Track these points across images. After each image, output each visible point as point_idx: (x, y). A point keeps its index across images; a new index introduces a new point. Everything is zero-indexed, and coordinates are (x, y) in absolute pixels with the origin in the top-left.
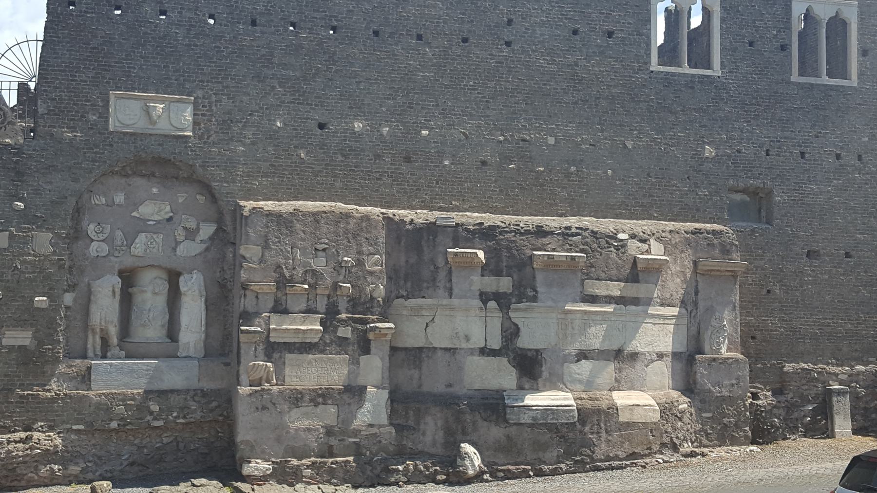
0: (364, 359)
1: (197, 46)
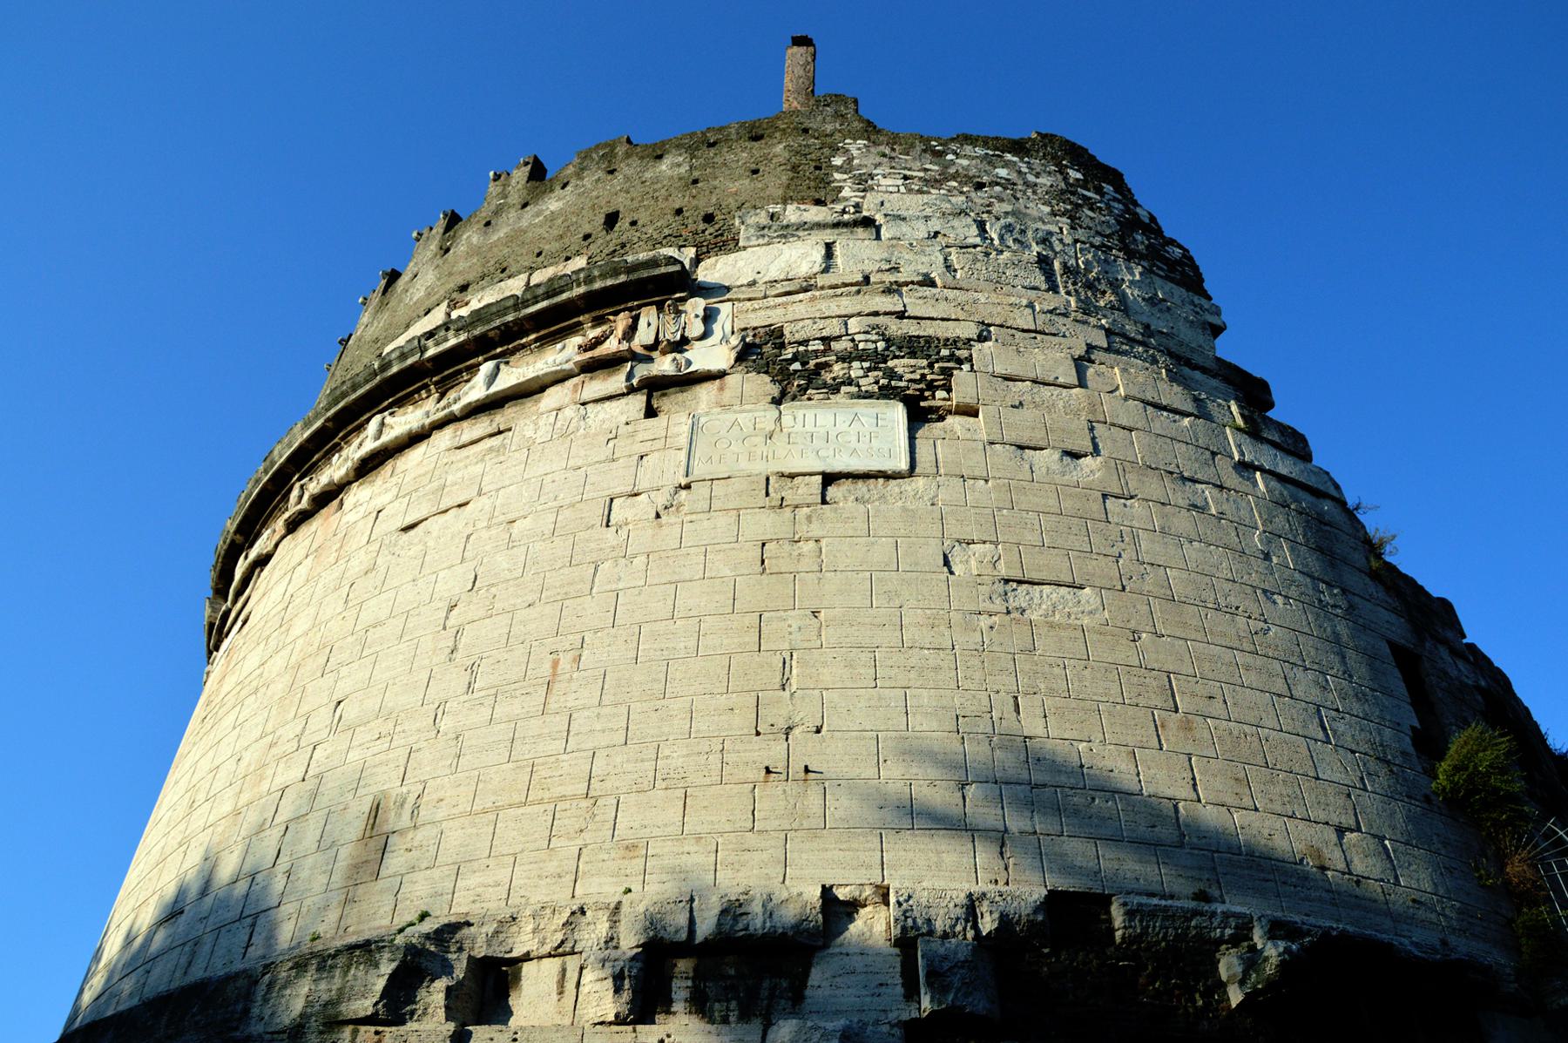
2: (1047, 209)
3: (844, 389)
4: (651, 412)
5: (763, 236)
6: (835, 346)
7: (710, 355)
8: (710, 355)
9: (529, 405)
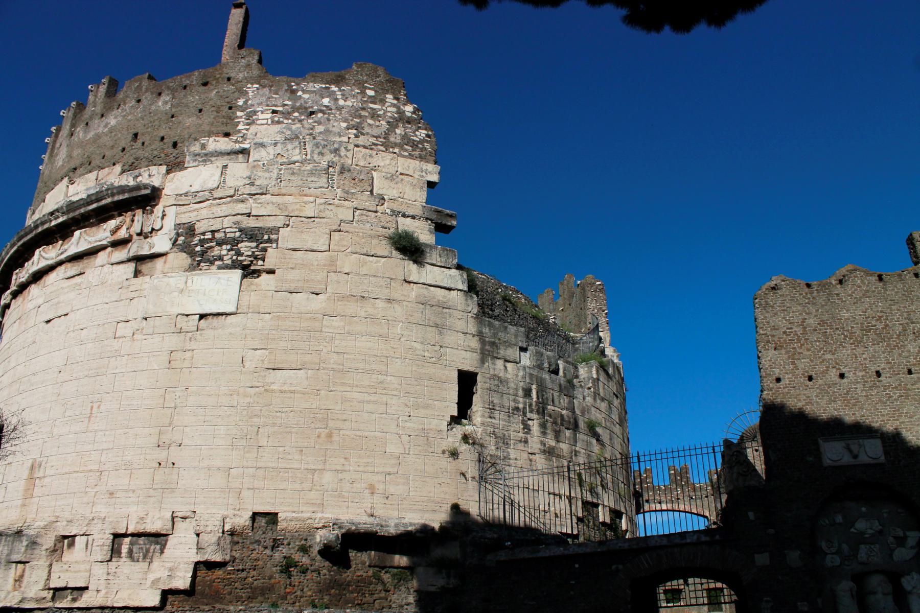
1: (872, 395)
2: (344, 125)
3: (217, 263)
4: (137, 273)
5: (196, 160)
6: (218, 235)
7: (160, 243)
8: (160, 243)
9: (92, 258)
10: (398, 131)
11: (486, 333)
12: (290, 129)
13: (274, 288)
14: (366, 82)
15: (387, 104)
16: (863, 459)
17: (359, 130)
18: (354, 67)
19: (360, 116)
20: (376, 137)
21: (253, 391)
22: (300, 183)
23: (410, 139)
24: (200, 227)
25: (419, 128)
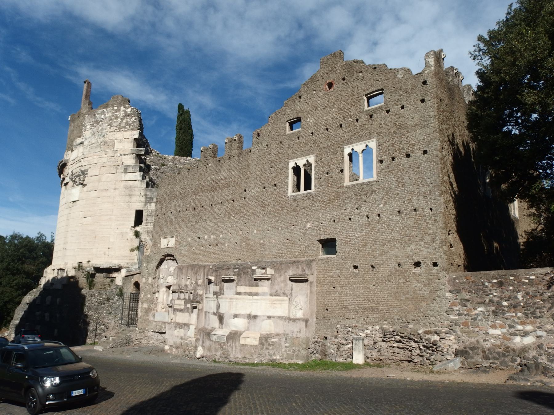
0: (192, 314)
3: (76, 184)
10: (124, 121)
11: (148, 194)
12: (93, 131)
13: (86, 191)
14: (115, 104)
15: (121, 111)
16: (170, 245)
17: (110, 125)
18: (112, 99)
19: (112, 119)
20: (116, 126)
21: (80, 225)
22: (93, 151)
23: (128, 123)
24: (74, 172)
25: (132, 117)
